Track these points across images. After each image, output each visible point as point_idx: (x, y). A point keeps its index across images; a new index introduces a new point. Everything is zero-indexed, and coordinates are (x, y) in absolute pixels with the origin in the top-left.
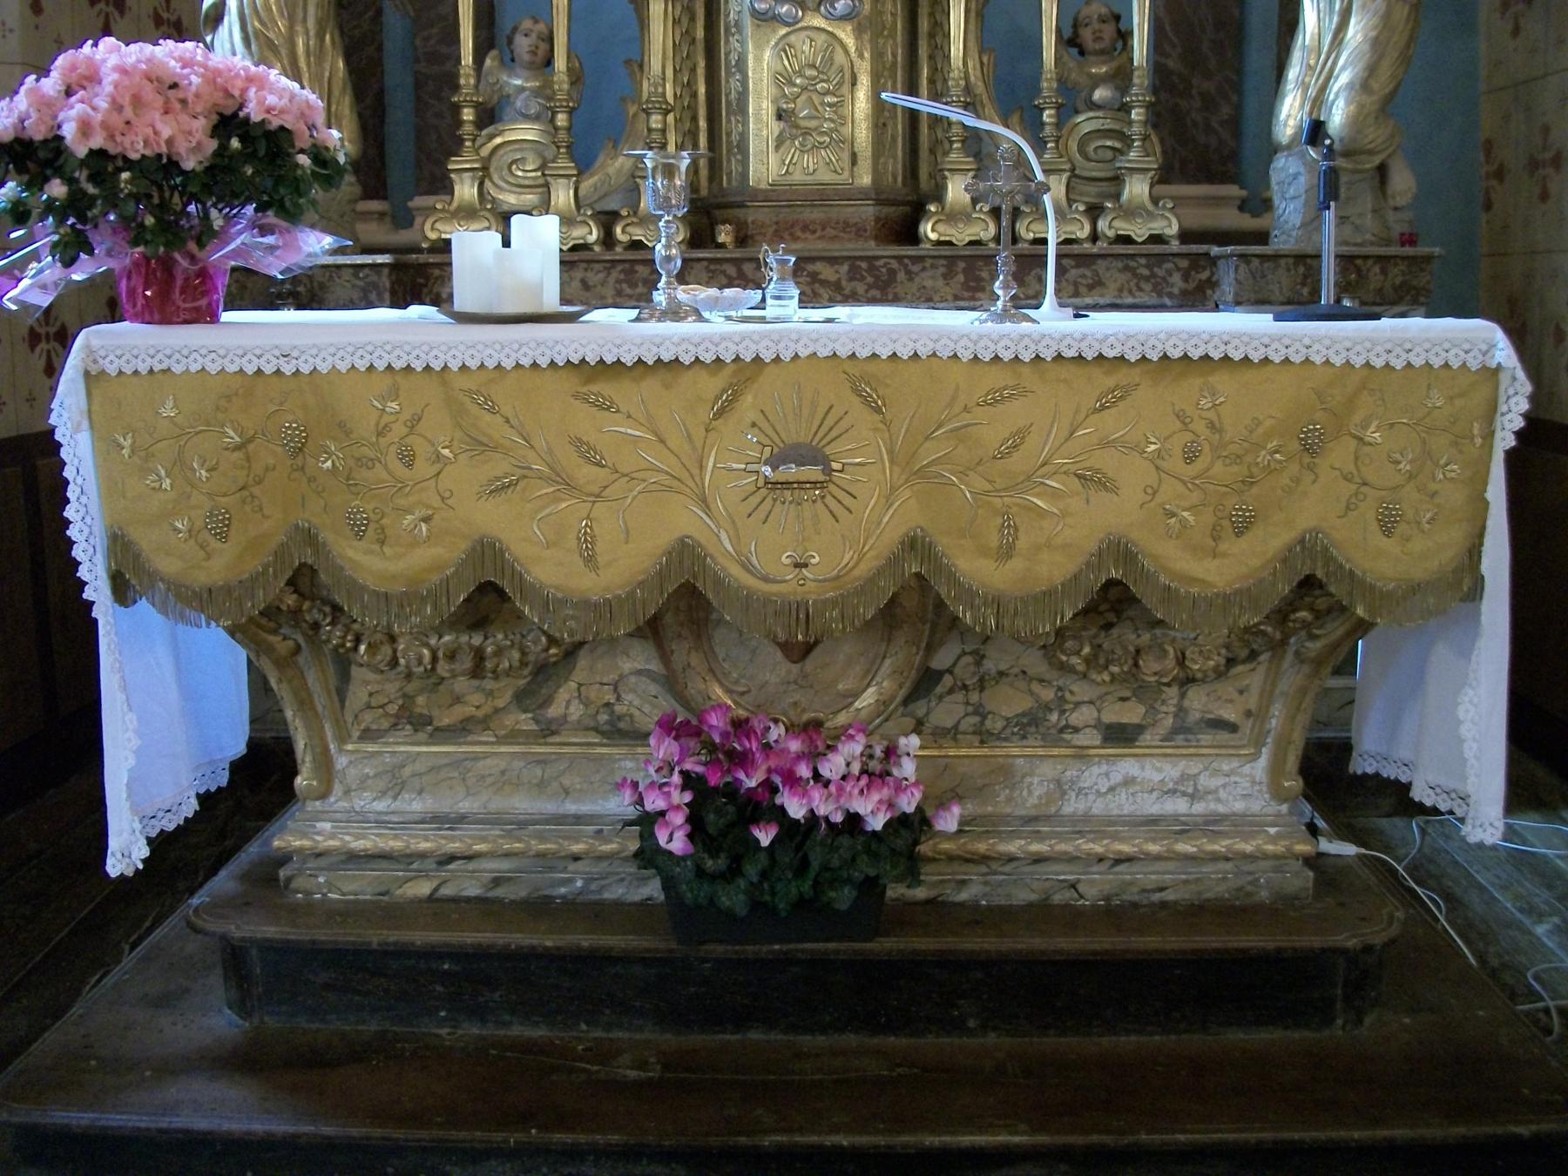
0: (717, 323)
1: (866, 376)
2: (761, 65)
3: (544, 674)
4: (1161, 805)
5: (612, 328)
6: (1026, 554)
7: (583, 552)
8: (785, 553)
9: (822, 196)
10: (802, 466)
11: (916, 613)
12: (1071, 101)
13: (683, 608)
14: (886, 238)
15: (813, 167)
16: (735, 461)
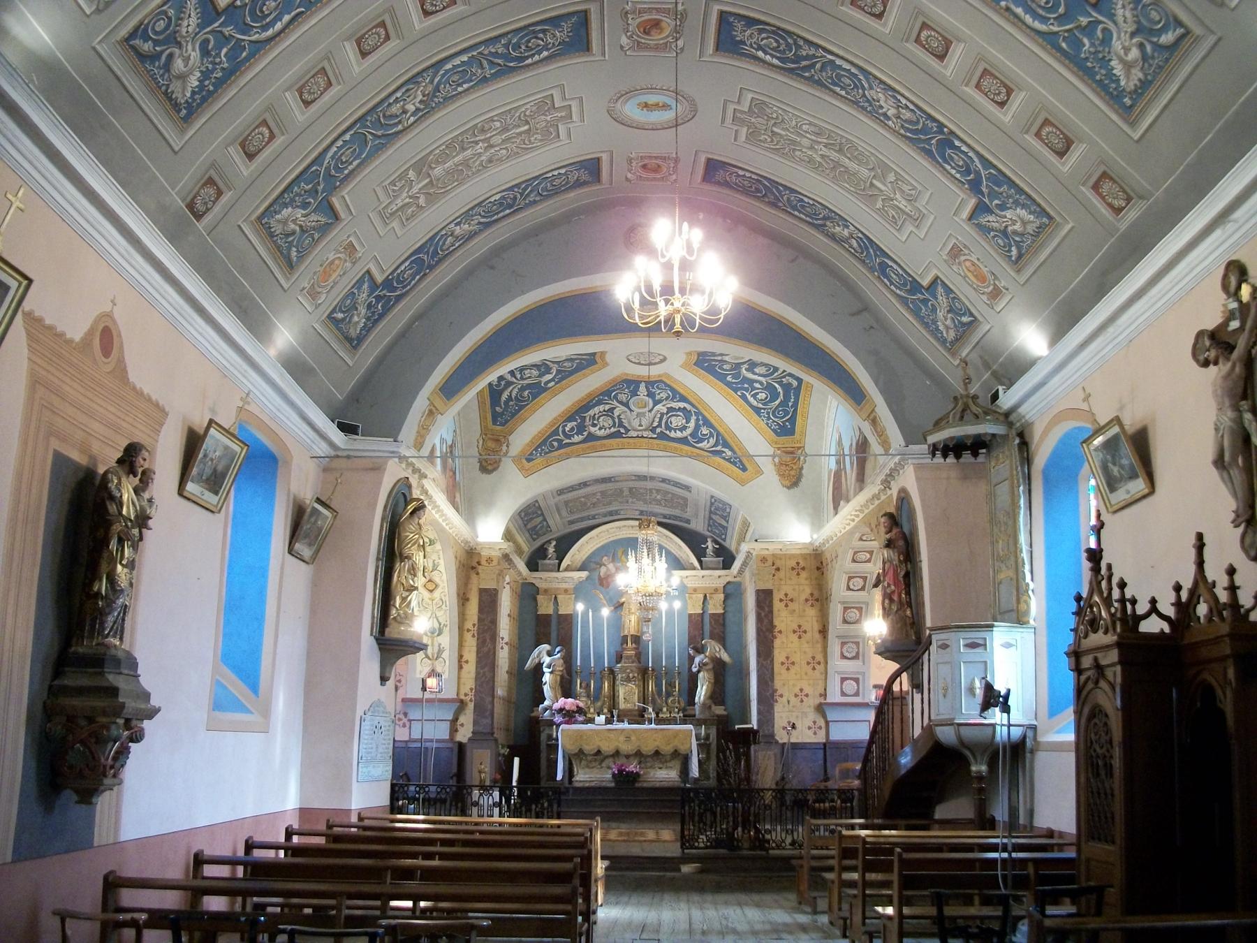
0: (620, 726)
1: (633, 730)
2: (621, 691)
3: (602, 761)
4: (667, 775)
5: (609, 726)
6: (648, 748)
7: (607, 748)
8: (626, 748)
9: (630, 711)
10: (628, 738)
11: (638, 754)
12: (669, 694)
13: (617, 754)
14: (640, 716)
15: (629, 706)
16: (622, 738)
